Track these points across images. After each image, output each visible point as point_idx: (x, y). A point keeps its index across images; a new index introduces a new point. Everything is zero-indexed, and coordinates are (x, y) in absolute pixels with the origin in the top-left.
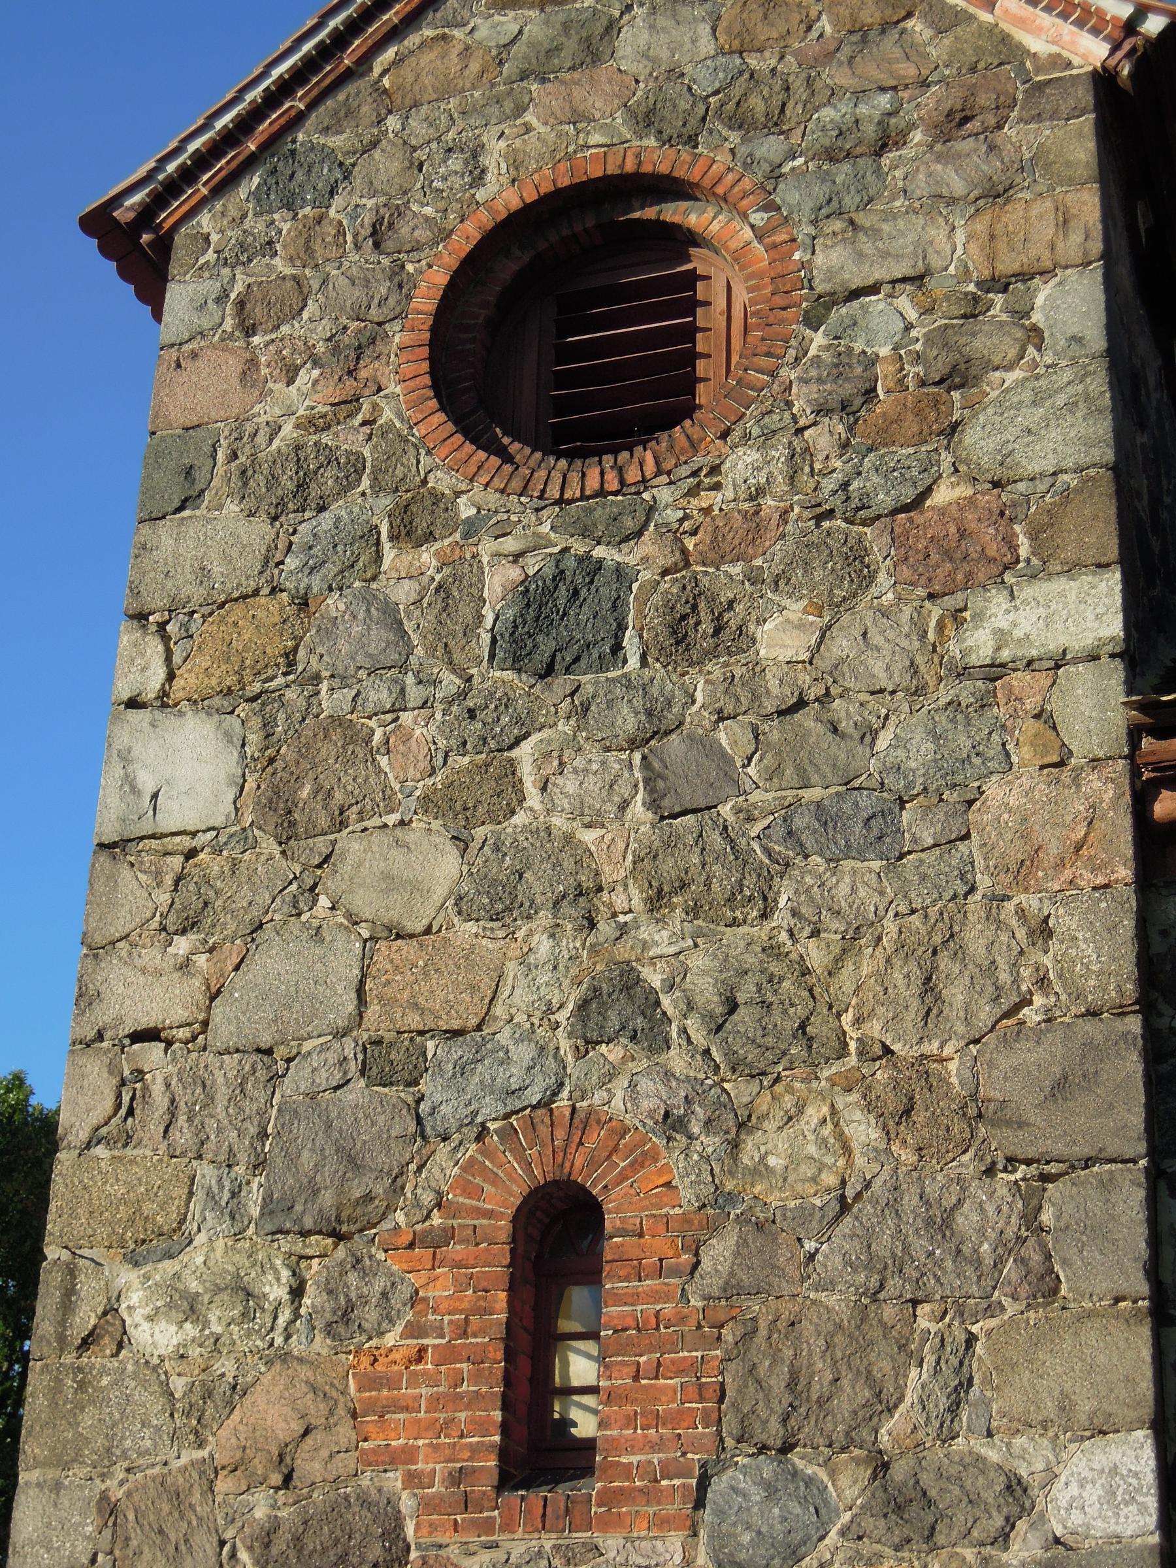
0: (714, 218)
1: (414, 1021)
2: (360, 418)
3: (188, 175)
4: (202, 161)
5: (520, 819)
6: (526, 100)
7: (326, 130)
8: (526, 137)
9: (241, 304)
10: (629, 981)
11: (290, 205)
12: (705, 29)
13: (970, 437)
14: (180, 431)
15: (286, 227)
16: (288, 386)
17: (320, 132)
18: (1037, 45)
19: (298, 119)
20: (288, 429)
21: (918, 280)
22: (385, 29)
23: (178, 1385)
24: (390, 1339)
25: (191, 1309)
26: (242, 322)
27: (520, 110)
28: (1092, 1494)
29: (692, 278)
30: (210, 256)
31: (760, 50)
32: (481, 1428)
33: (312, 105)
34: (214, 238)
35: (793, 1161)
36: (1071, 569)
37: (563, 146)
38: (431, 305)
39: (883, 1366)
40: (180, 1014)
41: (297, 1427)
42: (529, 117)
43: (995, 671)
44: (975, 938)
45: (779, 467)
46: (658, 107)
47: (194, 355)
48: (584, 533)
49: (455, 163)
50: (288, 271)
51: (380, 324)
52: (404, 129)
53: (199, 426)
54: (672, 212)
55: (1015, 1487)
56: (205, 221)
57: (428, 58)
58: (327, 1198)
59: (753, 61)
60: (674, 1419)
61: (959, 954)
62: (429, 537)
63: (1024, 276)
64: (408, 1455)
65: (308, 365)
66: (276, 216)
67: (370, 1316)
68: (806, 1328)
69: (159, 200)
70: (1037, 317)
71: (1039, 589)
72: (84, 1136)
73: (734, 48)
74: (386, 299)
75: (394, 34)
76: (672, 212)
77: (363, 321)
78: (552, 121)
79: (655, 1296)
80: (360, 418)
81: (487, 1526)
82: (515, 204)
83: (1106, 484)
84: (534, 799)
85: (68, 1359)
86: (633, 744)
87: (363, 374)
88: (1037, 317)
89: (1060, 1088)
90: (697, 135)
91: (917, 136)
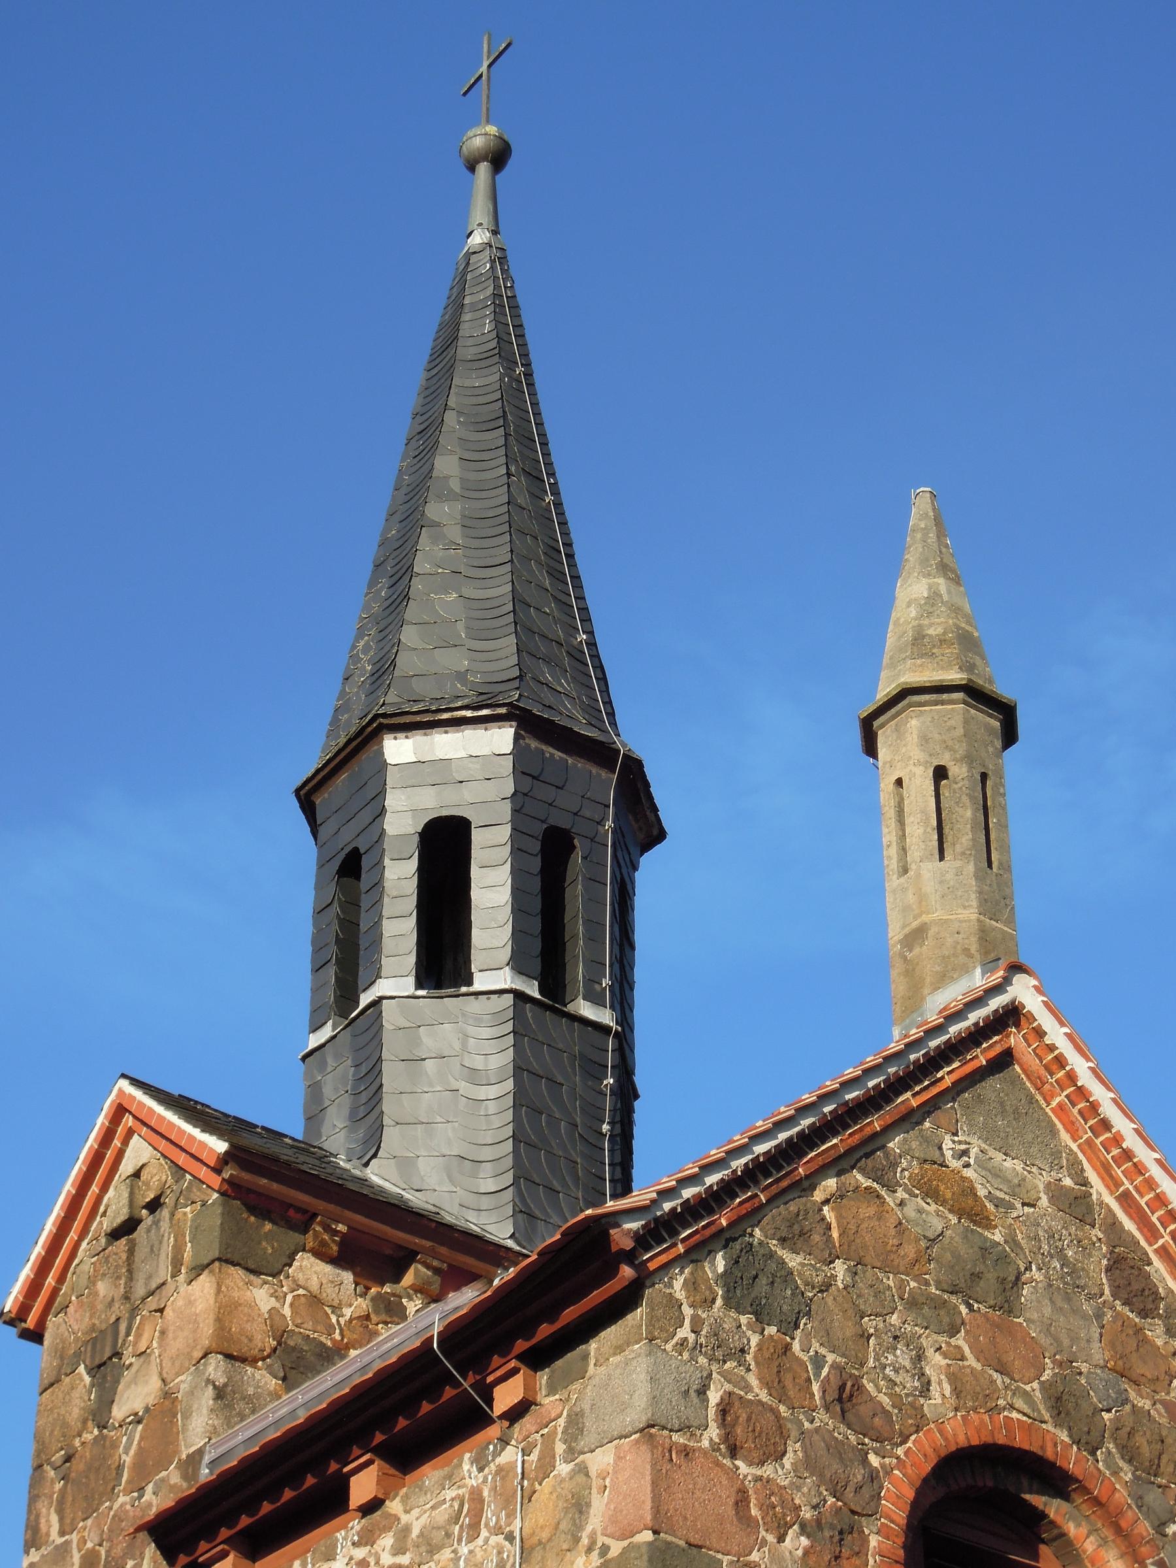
0: (1088, 1537)
6: (959, 1322)
7: (783, 1240)
8: (960, 1362)
9: (724, 1410)
11: (761, 1316)
12: (1095, 1331)
14: (682, 1543)
15: (755, 1340)
16: (779, 1542)
17: (778, 1240)
19: (754, 1214)
22: (833, 1154)
27: (953, 1331)
30: (685, 1332)
31: (1136, 1383)
34: (687, 1311)
37: (995, 1397)
38: (901, 1516)
42: (960, 1340)
46: (1065, 1397)
47: (686, 1452)
49: (903, 1356)
50: (764, 1396)
51: (853, 1512)
52: (853, 1286)
53: (700, 1547)
57: (868, 1210)
59: (1132, 1394)
65: (796, 1527)
66: (744, 1319)
69: (645, 1240)
73: (1118, 1369)
74: (861, 1488)
75: (839, 1164)
77: (838, 1500)
78: (982, 1359)
82: (962, 1441)
90: (1097, 1449)
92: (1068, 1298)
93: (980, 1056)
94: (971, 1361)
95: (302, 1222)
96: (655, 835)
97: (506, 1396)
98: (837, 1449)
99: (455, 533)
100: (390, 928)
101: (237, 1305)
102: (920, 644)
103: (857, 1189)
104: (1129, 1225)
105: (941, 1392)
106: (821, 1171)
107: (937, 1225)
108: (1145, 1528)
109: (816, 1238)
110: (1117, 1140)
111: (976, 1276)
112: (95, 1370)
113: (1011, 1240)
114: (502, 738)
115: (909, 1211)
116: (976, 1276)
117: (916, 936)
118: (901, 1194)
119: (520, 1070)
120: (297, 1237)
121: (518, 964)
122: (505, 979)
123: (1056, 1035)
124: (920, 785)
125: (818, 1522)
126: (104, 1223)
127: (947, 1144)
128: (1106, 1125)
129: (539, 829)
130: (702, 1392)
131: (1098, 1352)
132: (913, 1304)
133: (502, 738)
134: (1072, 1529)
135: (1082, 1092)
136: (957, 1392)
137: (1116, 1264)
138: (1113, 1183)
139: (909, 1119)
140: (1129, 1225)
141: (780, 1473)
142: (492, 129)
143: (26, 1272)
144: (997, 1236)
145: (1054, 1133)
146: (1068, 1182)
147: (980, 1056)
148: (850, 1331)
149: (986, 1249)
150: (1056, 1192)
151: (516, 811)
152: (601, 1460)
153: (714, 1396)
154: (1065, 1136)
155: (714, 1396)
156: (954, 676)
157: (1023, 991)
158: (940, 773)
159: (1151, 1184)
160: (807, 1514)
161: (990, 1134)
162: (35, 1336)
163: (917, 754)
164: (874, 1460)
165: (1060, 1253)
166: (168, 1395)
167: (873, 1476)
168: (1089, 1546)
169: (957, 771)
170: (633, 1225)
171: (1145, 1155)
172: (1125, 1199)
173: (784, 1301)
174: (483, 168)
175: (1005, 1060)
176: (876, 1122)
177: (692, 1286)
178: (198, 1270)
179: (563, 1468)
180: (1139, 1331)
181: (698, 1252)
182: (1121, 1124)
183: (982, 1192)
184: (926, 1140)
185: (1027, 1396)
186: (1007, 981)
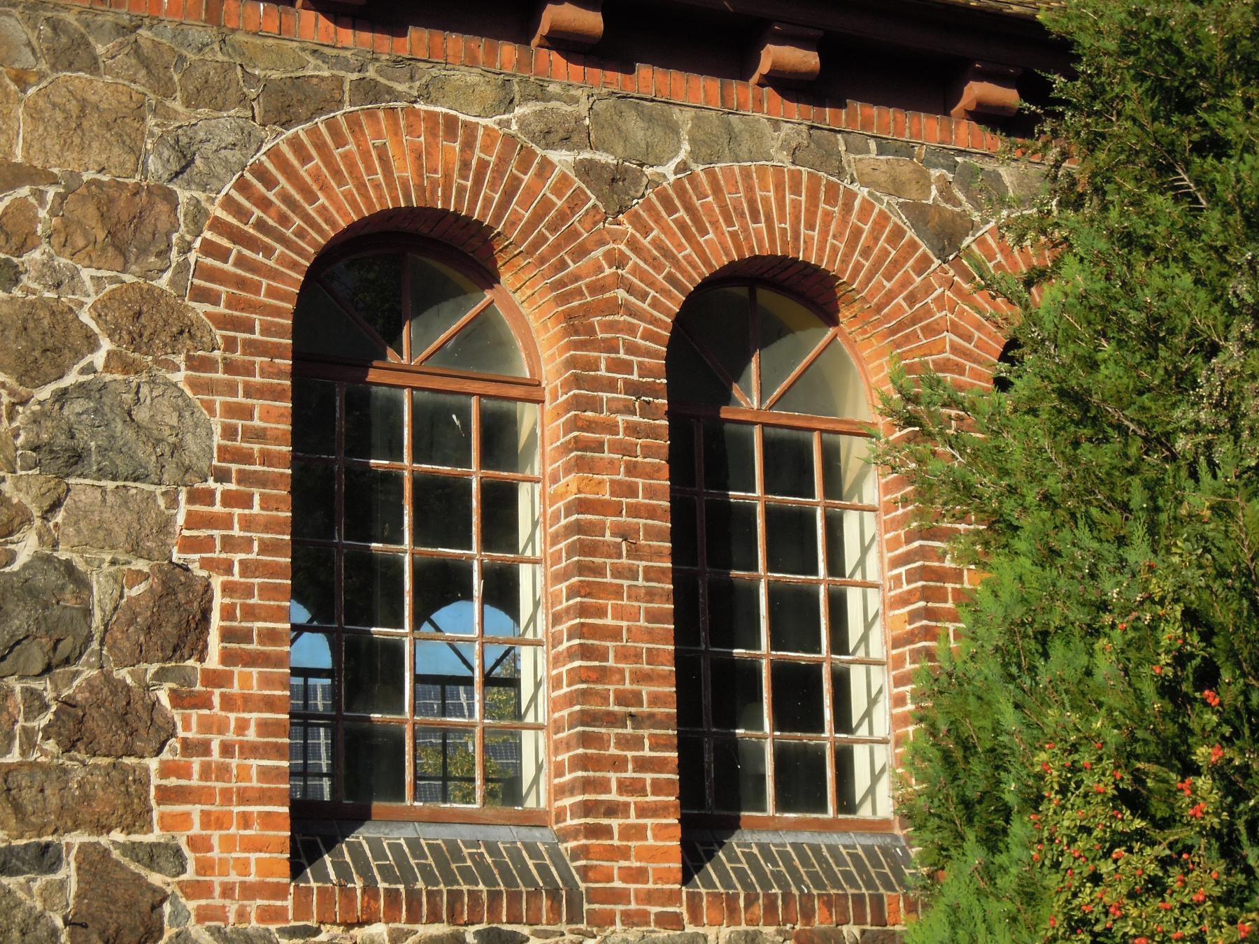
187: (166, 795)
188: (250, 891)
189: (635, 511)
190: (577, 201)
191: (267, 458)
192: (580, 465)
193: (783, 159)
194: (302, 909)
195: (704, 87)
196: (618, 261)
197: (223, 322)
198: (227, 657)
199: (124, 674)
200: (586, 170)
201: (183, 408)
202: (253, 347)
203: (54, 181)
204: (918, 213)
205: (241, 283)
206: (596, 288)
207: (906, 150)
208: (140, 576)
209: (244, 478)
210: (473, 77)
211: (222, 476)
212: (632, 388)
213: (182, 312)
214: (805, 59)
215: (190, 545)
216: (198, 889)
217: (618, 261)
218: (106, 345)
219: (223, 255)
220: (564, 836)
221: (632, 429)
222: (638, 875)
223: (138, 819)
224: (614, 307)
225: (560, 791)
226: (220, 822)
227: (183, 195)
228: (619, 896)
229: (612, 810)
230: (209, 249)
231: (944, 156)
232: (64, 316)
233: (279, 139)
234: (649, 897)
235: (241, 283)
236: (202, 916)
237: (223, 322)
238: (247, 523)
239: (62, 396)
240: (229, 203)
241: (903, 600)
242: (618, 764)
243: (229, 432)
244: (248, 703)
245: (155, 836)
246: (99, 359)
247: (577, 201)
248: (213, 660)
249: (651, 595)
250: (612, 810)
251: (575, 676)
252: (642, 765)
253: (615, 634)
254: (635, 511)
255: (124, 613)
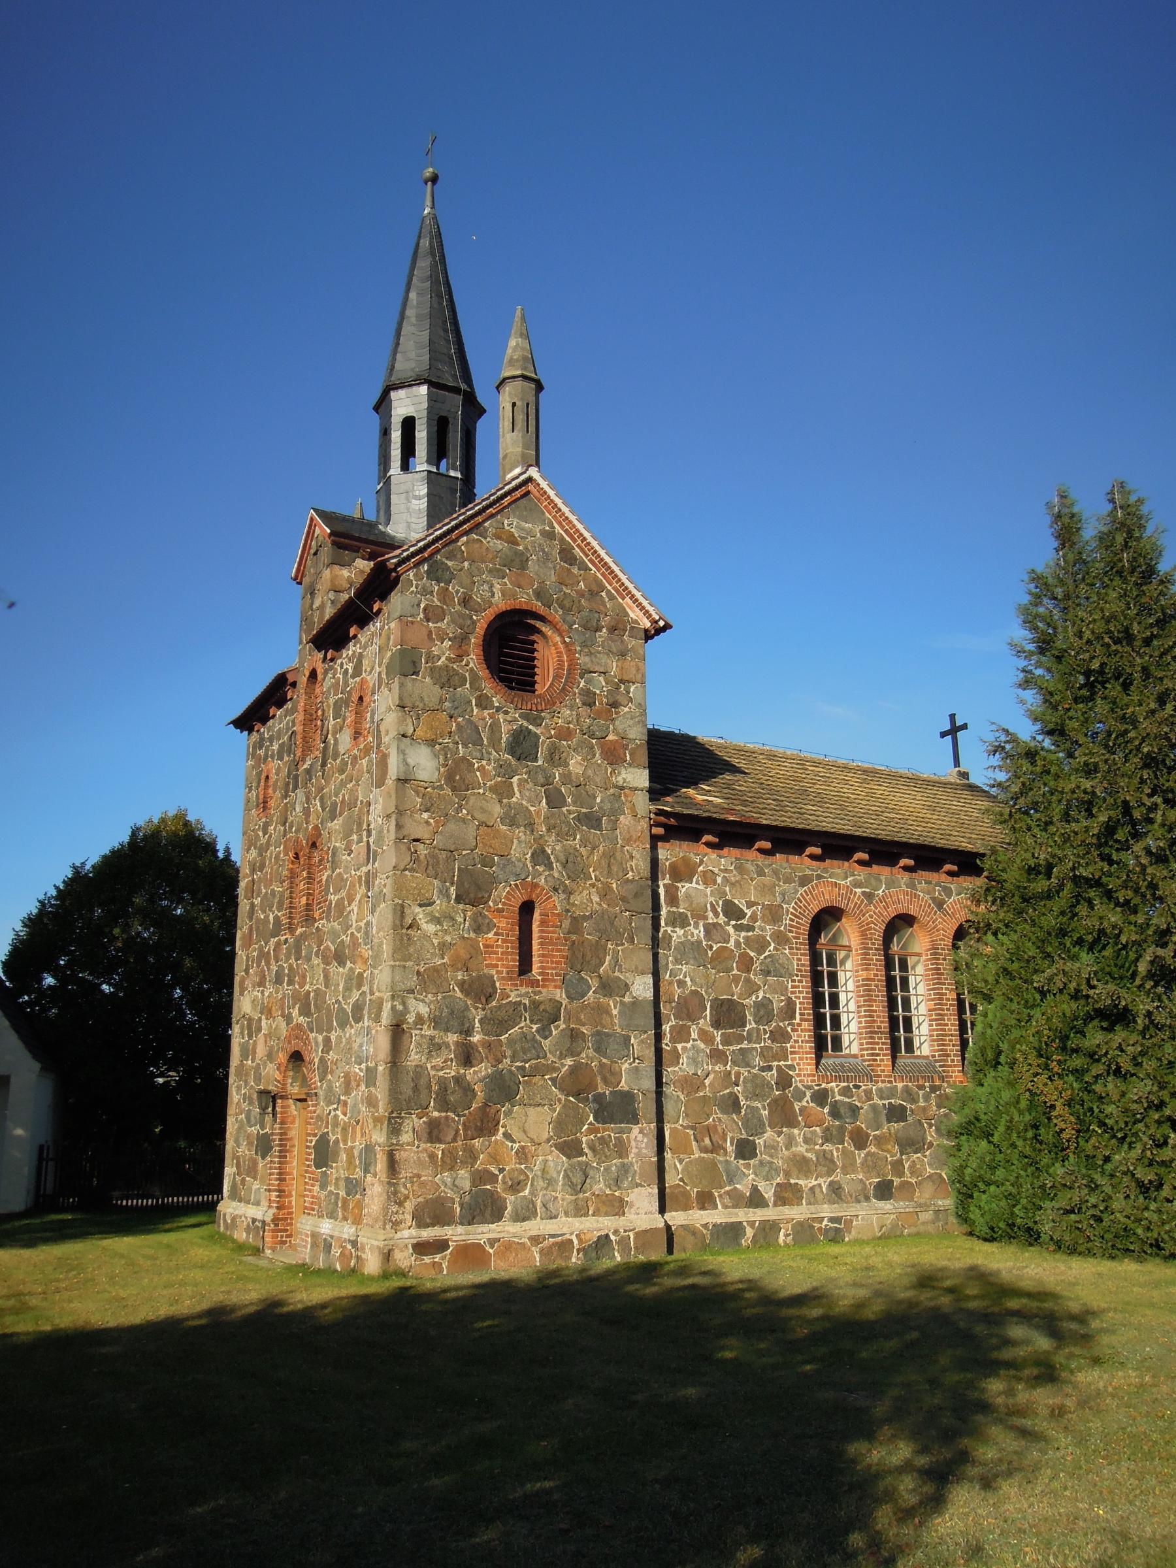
1: (491, 851)
2: (464, 663)
3: (408, 558)
4: (413, 555)
5: (514, 799)
7: (447, 558)
9: (425, 609)
10: (544, 851)
11: (438, 581)
13: (617, 723)
15: (436, 588)
18: (632, 615)
19: (438, 551)
20: (443, 659)
21: (604, 673)
23: (436, 942)
24: (490, 935)
25: (438, 921)
26: (425, 617)
27: (503, 578)
28: (641, 988)
29: (533, 642)
30: (413, 589)
32: (514, 960)
33: (443, 548)
34: (414, 582)
35: (582, 903)
36: (638, 766)
38: (482, 633)
39: (601, 955)
40: (426, 836)
41: (469, 956)
42: (506, 580)
43: (622, 788)
44: (618, 855)
45: (574, 717)
47: (412, 623)
48: (528, 721)
49: (486, 587)
50: (439, 604)
54: (538, 624)
55: (626, 985)
56: (411, 574)
57: (477, 546)
58: (472, 896)
59: (564, 589)
60: (557, 963)
61: (615, 859)
62: (486, 708)
63: (629, 682)
64: (496, 966)
67: (485, 929)
68: (585, 944)
69: (399, 564)
70: (631, 695)
71: (631, 770)
72: (402, 867)
75: (466, 533)
76: (538, 624)
79: (554, 932)
80: (464, 663)
81: (516, 985)
82: (504, 609)
83: (646, 747)
84: (517, 794)
85: (404, 931)
86: (543, 786)
87: (464, 648)
88: (631, 695)
89: (636, 895)
91: (604, 630)
92: (544, 563)
93: (518, 494)
94: (509, 586)
95: (358, 551)
96: (482, 411)
97: (376, 608)
98: (461, 615)
99: (413, 320)
100: (393, 453)
101: (337, 576)
102: (512, 362)
103: (474, 539)
104: (568, 539)
105: (498, 595)
106: (462, 536)
107: (501, 547)
108: (565, 627)
109: (459, 556)
110: (563, 514)
111: (512, 561)
112: (311, 594)
113: (526, 549)
114: (424, 389)
115: (491, 544)
116: (512, 561)
117: (505, 457)
118: (488, 539)
119: (429, 495)
120: (355, 554)
121: (429, 462)
122: (425, 467)
123: (544, 484)
124: (509, 407)
125: (455, 637)
126: (312, 551)
127: (506, 522)
128: (560, 510)
129: (436, 417)
130: (419, 605)
131: (553, 578)
132: (490, 571)
133: (424, 389)
134: (544, 629)
135: (552, 501)
136: (503, 595)
137: (562, 551)
138: (562, 527)
139: (492, 516)
140: (568, 539)
141: (442, 625)
142: (431, 170)
143: (296, 566)
144: (521, 548)
145: (543, 513)
146: (547, 528)
147: (518, 494)
148: (469, 581)
149: (516, 553)
150: (543, 532)
151: (428, 413)
152: (392, 625)
153: (422, 606)
154: (547, 514)
155: (422, 606)
156: (519, 372)
157: (533, 472)
158: (514, 404)
159: (574, 526)
160: (451, 635)
161: (521, 518)
162: (300, 583)
163: (507, 399)
164: (474, 617)
165: (543, 551)
166: (322, 602)
167: (474, 623)
168: (549, 633)
169: (518, 403)
170: (394, 561)
171: (573, 518)
172: (566, 531)
173: (447, 575)
174: (429, 183)
175: (528, 493)
176: (479, 519)
177: (415, 575)
178: (328, 566)
179: (386, 627)
180: (569, 570)
181: (417, 565)
182: (565, 509)
183: (516, 535)
184: (498, 522)
185: (528, 594)
186: (527, 470)
187: (792, 1053)
188: (809, 1075)
189: (878, 980)
190: (862, 901)
191: (805, 971)
192: (867, 969)
193: (904, 887)
194: (819, 1080)
195: (887, 869)
196: (871, 917)
197: (795, 938)
198: (801, 1020)
199: (781, 1024)
200: (864, 893)
201: (788, 959)
202: (801, 944)
203: (759, 904)
204: (933, 899)
205: (798, 928)
206: (867, 924)
207: (930, 883)
208: (782, 1001)
209: (801, 976)
210: (839, 871)
211: (797, 976)
212: (876, 949)
213: (785, 935)
214: (911, 862)
215: (792, 993)
216: (799, 1075)
217: (871, 917)
218: (773, 945)
219: (793, 921)
220: (865, 1061)
221: (877, 960)
222: (883, 1071)
223: (786, 1059)
224: (871, 929)
225: (862, 1050)
226: (800, 1059)
227: (785, 906)
228: (880, 1076)
229: (878, 1055)
230: (791, 920)
231: (938, 884)
232: (764, 937)
233: (801, 891)
234: (886, 1076)
235: (798, 928)
236: (801, 1081)
237: (795, 938)
238: (803, 987)
239: (765, 957)
240: (793, 908)
241: (932, 1000)
242: (878, 1044)
243: (798, 965)
244: (806, 1030)
245: (789, 1063)
246: (771, 948)
247: (862, 901)
248: (797, 1021)
249: (882, 1001)
250: (878, 1055)
251: (866, 1022)
252: (883, 1044)
253: (875, 1011)
254: (878, 980)
255: (781, 1010)
